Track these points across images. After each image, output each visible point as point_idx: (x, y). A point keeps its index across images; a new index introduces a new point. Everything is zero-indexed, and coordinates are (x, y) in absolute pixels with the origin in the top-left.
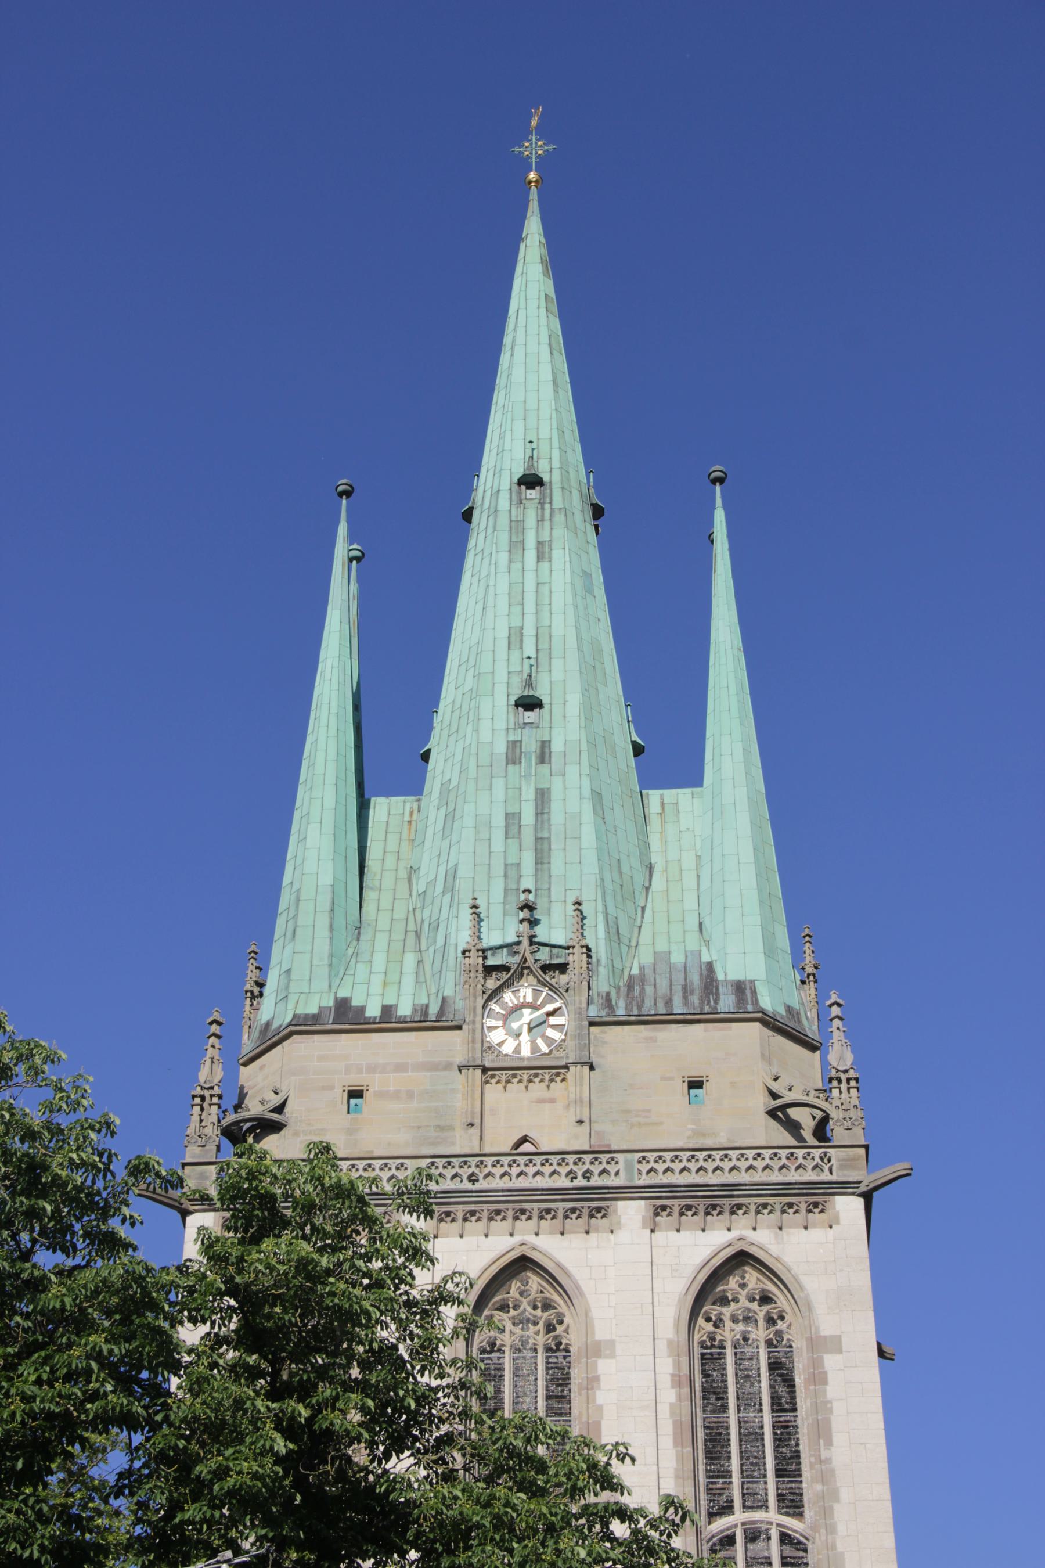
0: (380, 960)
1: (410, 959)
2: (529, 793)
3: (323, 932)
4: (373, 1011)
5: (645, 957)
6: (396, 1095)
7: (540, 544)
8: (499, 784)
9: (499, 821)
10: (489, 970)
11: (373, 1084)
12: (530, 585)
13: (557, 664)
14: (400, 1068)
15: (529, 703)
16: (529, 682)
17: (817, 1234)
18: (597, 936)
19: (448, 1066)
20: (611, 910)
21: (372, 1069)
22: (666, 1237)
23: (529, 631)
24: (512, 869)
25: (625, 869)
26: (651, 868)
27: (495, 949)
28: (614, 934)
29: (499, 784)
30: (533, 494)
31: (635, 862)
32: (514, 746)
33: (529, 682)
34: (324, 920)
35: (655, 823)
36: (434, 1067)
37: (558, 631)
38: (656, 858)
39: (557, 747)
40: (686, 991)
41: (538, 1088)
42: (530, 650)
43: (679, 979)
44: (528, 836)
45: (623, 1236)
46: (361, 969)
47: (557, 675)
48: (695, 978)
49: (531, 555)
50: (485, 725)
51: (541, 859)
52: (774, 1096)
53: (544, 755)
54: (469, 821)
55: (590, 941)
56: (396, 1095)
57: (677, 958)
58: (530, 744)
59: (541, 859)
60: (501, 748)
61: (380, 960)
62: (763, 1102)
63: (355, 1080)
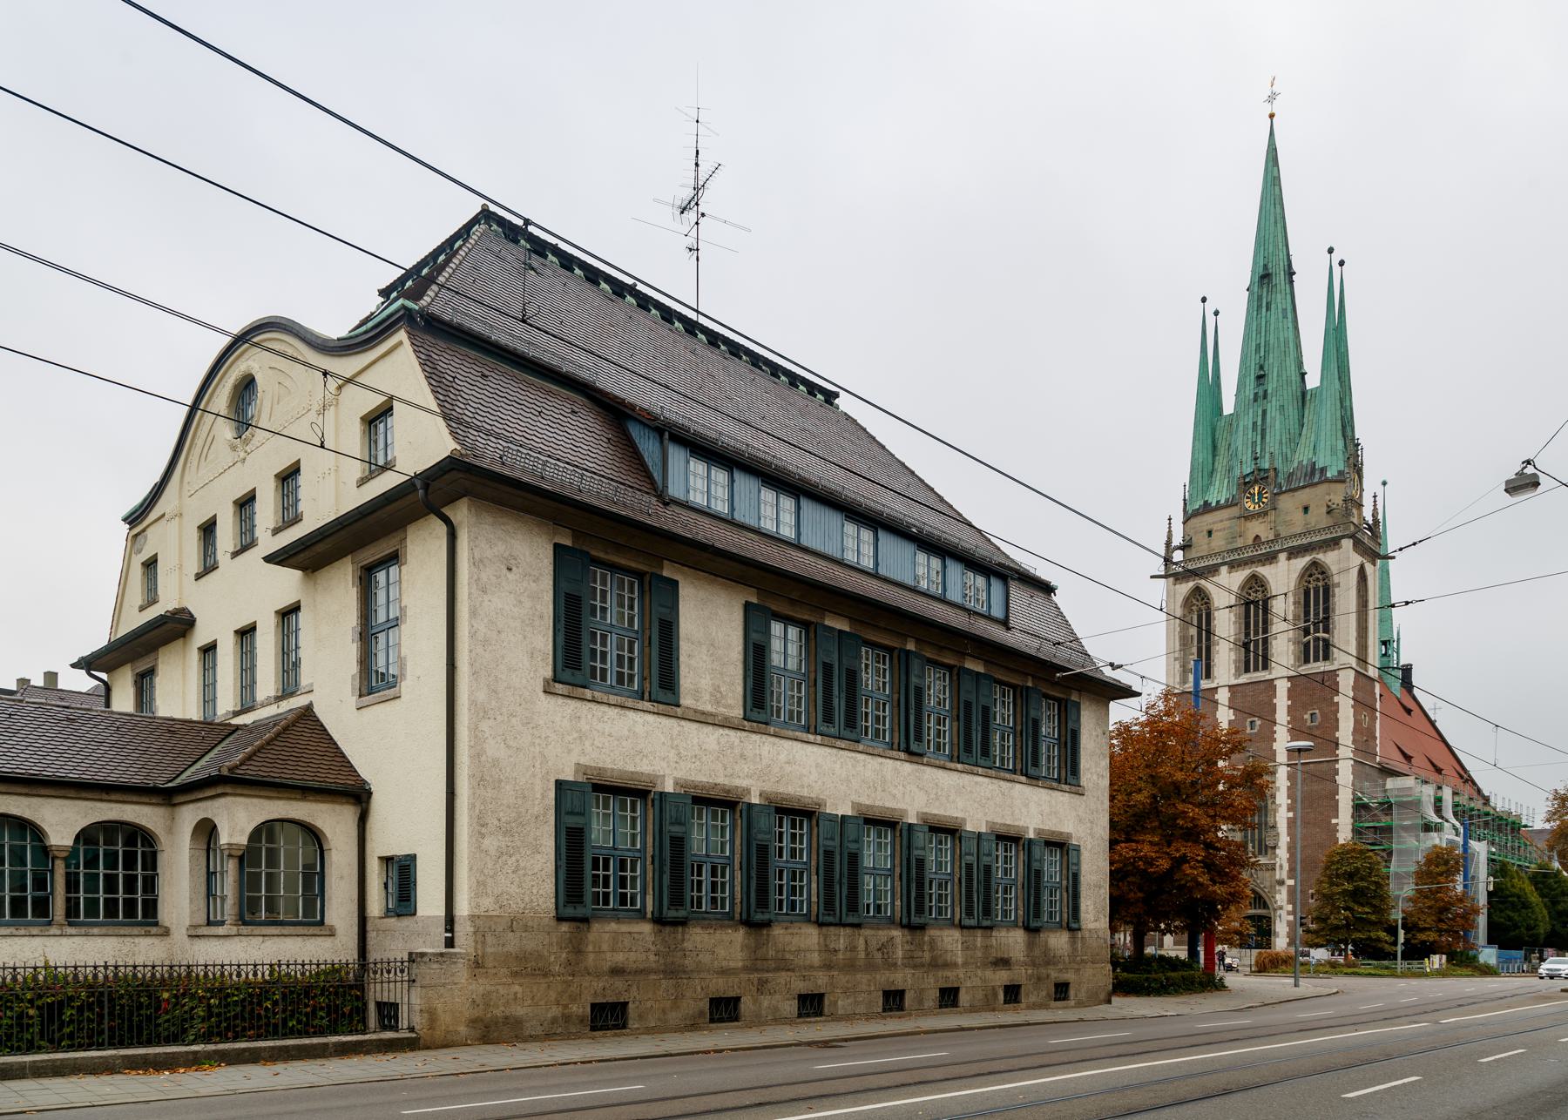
0: (1217, 482)
1: (1226, 481)
2: (1260, 413)
3: (1200, 479)
4: (1214, 504)
5: (1296, 465)
6: (1220, 530)
7: (1267, 303)
8: (1251, 411)
9: (1251, 426)
10: (1245, 483)
11: (1215, 527)
12: (1263, 324)
13: (1271, 355)
14: (1222, 521)
15: (1260, 378)
16: (1261, 367)
17: (1336, 552)
18: (1279, 464)
19: (1234, 518)
20: (1284, 450)
21: (1214, 523)
22: (1293, 561)
23: (1262, 345)
24: (1254, 443)
25: (1292, 431)
26: (1303, 426)
27: (1248, 475)
28: (1286, 459)
29: (1251, 411)
30: (1266, 281)
31: (1297, 426)
32: (1256, 394)
33: (1261, 367)
34: (1200, 474)
35: (1308, 403)
36: (1230, 519)
37: (1271, 342)
38: (1306, 420)
39: (1269, 391)
40: (1306, 475)
41: (1260, 520)
42: (1262, 354)
43: (1304, 470)
44: (1259, 428)
45: (1280, 564)
46: (1212, 488)
47: (1271, 361)
48: (1309, 469)
49: (1264, 310)
50: (1248, 388)
51: (1263, 437)
52: (1328, 506)
53: (1265, 396)
54: (1241, 428)
55: (1276, 466)
56: (1220, 530)
57: (1305, 463)
58: (1261, 394)
59: (1263, 437)
60: (1252, 397)
61: (1217, 482)
62: (1324, 509)
63: (1209, 527)
